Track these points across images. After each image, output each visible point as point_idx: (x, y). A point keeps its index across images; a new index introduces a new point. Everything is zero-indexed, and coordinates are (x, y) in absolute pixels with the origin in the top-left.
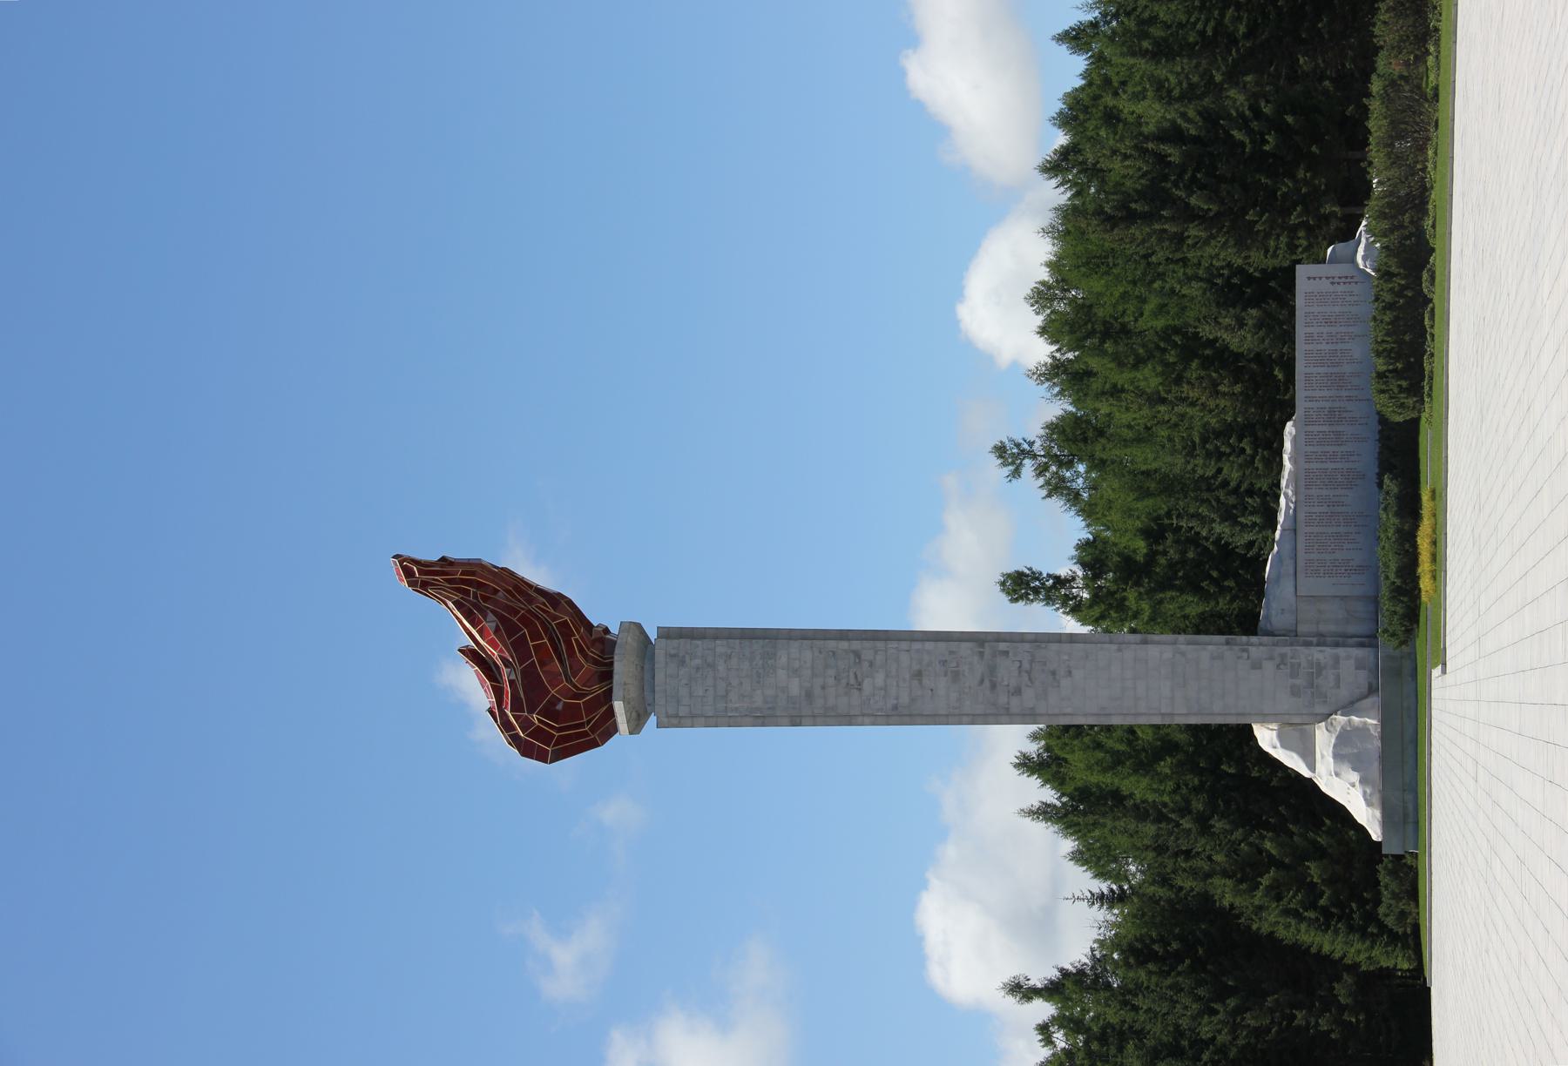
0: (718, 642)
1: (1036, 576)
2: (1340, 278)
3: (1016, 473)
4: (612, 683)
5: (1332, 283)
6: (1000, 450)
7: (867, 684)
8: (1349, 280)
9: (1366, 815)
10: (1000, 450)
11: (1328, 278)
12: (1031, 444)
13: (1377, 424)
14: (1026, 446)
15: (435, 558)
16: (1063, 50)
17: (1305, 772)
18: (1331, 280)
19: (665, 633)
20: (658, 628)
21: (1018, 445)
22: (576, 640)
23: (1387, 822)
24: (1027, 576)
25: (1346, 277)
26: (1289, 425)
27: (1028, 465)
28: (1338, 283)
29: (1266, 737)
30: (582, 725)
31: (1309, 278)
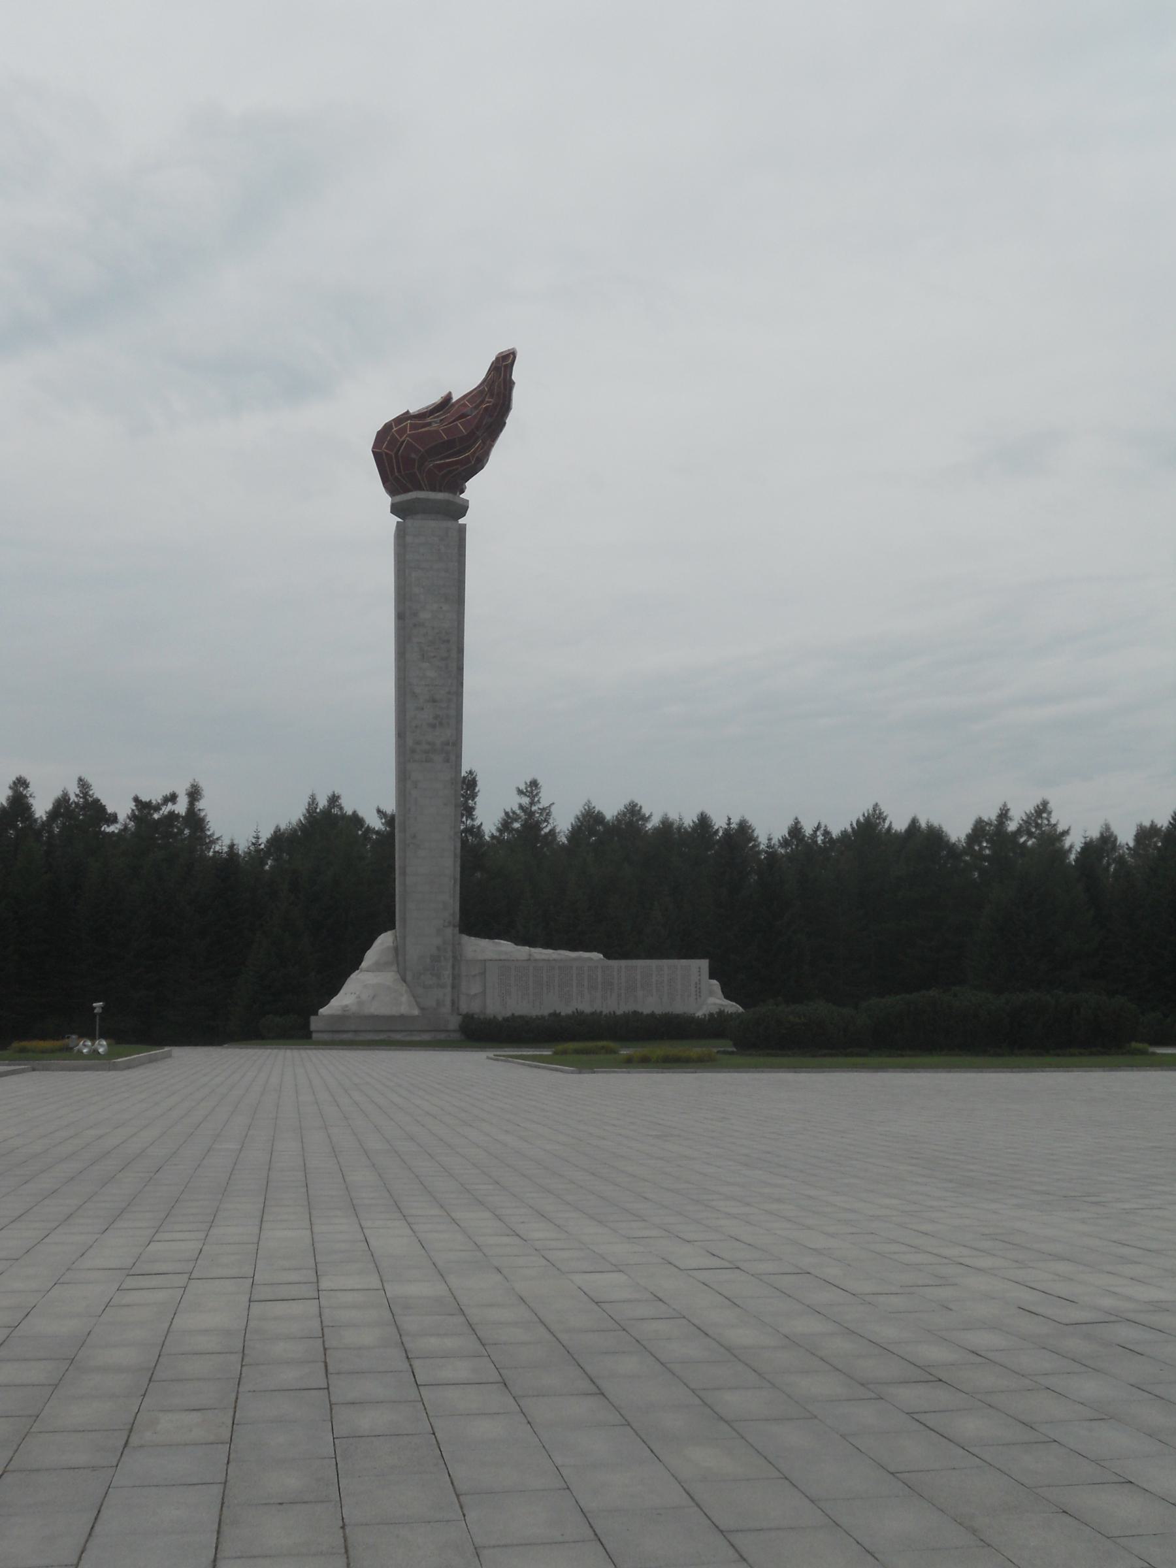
0: (456, 564)
1: (473, 796)
2: (700, 988)
3: (520, 792)
4: (427, 490)
5: (696, 983)
6: (534, 784)
7: (426, 665)
8: (698, 994)
9: (344, 1000)
10: (534, 784)
11: (700, 980)
12: (539, 801)
13: (633, 1010)
14: (536, 799)
15: (515, 376)
16: (791, 822)
17: (364, 965)
18: (698, 982)
19: (462, 529)
20: (466, 525)
21: (537, 794)
22: (457, 469)
23: (343, 1018)
24: (474, 789)
25: (700, 992)
26: (601, 956)
27: (525, 801)
28: (696, 987)
29: (384, 941)
30: (399, 471)
31: (700, 968)
